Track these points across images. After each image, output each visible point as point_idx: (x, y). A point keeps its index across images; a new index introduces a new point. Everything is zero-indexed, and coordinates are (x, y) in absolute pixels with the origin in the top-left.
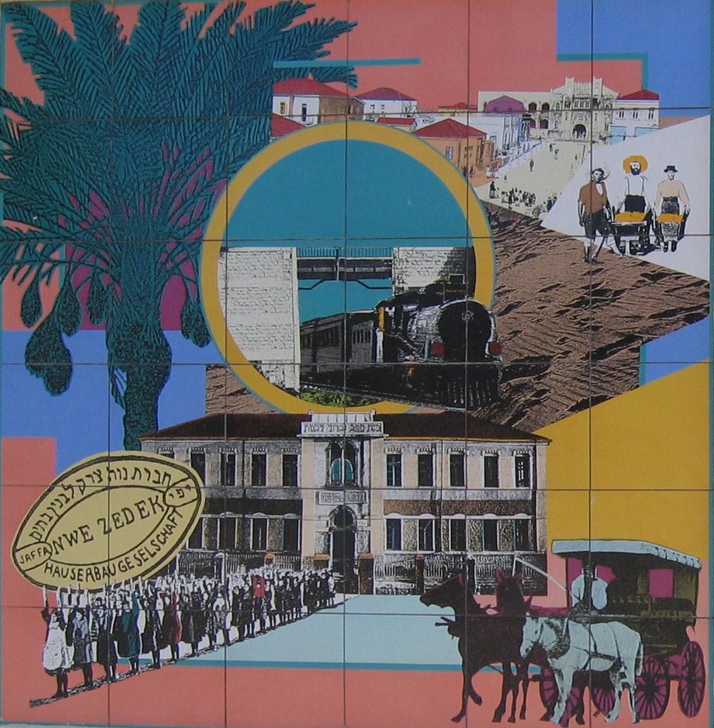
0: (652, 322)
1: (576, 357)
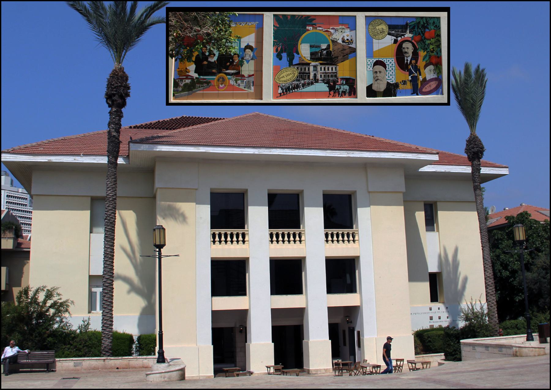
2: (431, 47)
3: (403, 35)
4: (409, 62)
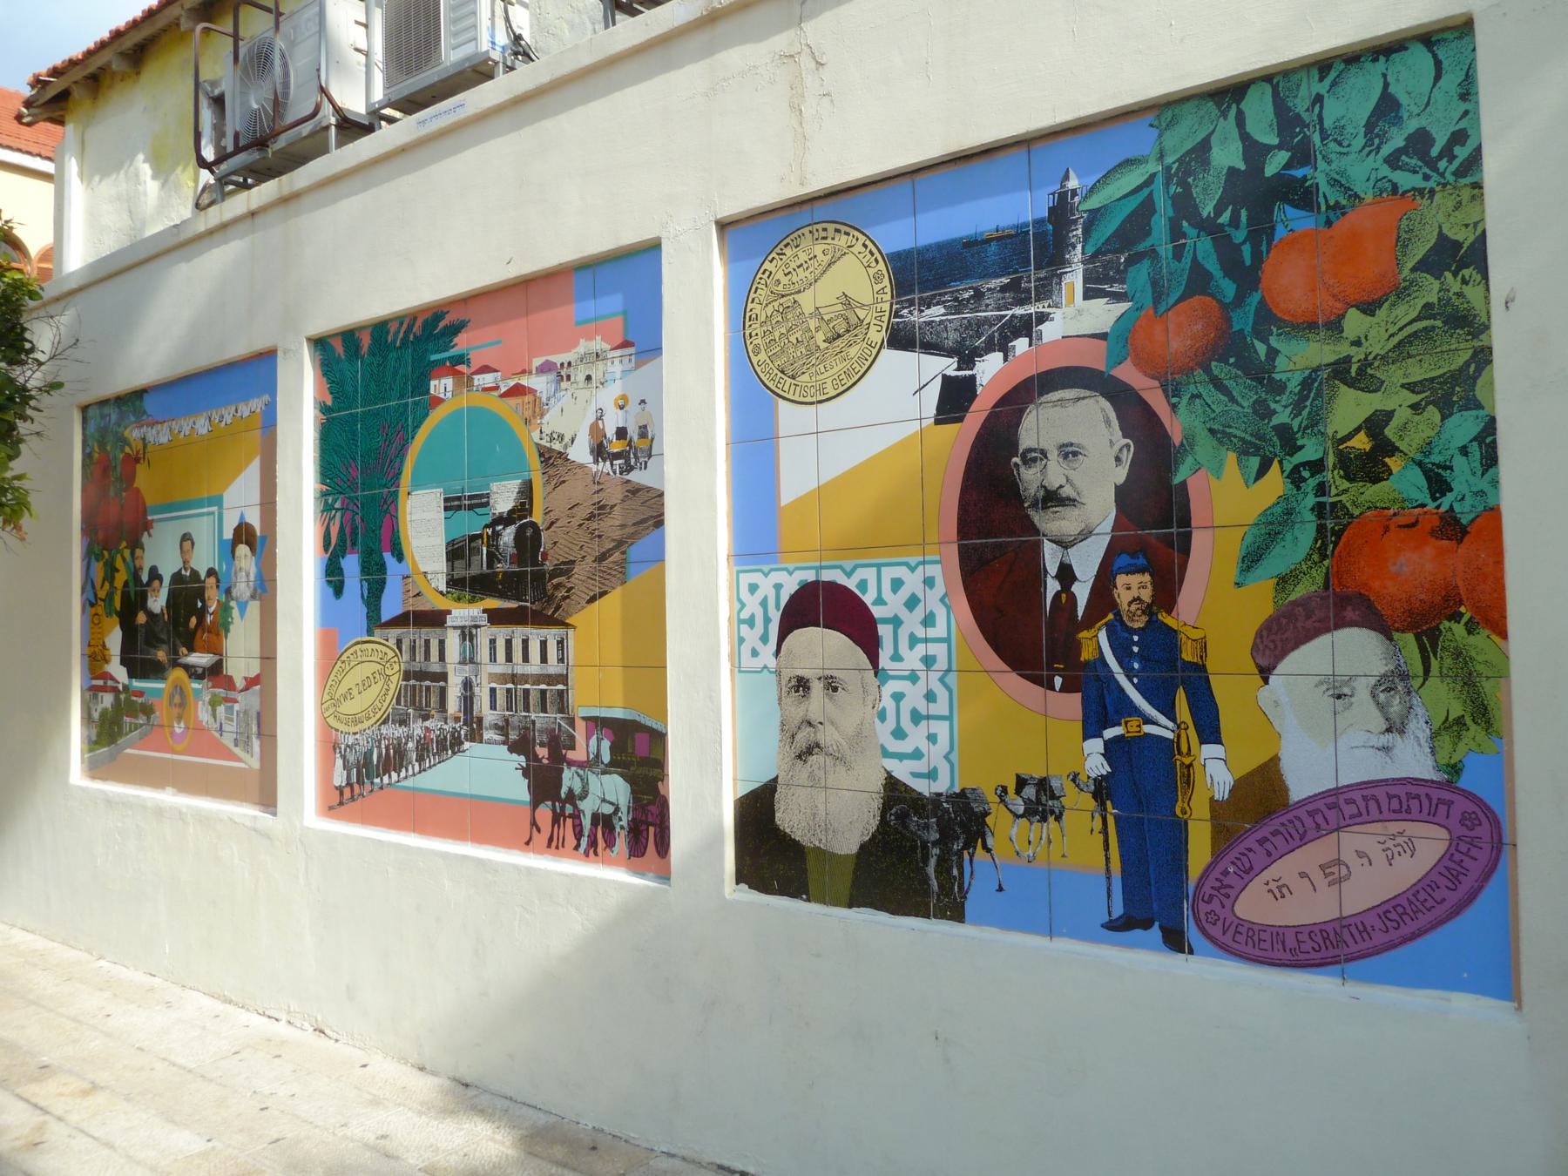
0: (632, 529)
1: (589, 559)
2: (1348, 410)
3: (1025, 327)
4: (1082, 591)
